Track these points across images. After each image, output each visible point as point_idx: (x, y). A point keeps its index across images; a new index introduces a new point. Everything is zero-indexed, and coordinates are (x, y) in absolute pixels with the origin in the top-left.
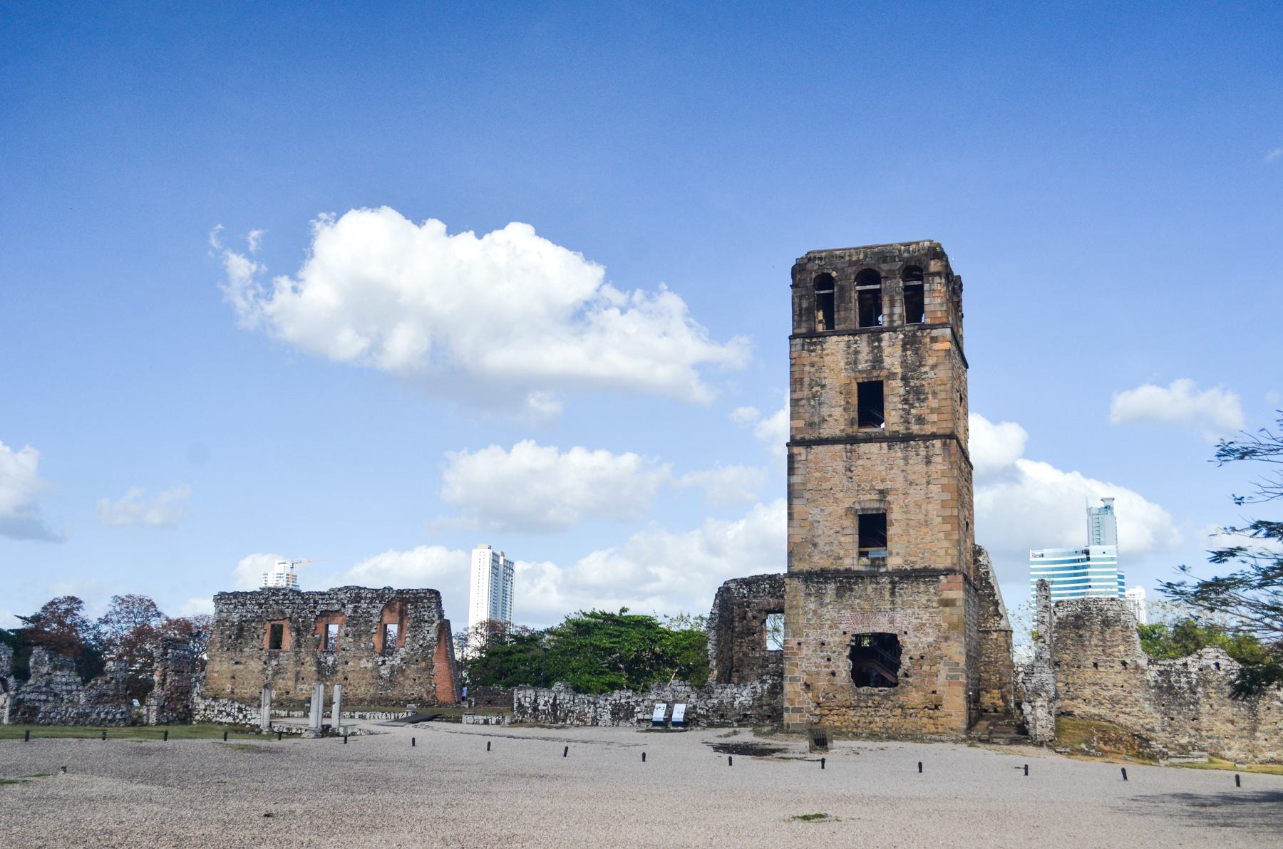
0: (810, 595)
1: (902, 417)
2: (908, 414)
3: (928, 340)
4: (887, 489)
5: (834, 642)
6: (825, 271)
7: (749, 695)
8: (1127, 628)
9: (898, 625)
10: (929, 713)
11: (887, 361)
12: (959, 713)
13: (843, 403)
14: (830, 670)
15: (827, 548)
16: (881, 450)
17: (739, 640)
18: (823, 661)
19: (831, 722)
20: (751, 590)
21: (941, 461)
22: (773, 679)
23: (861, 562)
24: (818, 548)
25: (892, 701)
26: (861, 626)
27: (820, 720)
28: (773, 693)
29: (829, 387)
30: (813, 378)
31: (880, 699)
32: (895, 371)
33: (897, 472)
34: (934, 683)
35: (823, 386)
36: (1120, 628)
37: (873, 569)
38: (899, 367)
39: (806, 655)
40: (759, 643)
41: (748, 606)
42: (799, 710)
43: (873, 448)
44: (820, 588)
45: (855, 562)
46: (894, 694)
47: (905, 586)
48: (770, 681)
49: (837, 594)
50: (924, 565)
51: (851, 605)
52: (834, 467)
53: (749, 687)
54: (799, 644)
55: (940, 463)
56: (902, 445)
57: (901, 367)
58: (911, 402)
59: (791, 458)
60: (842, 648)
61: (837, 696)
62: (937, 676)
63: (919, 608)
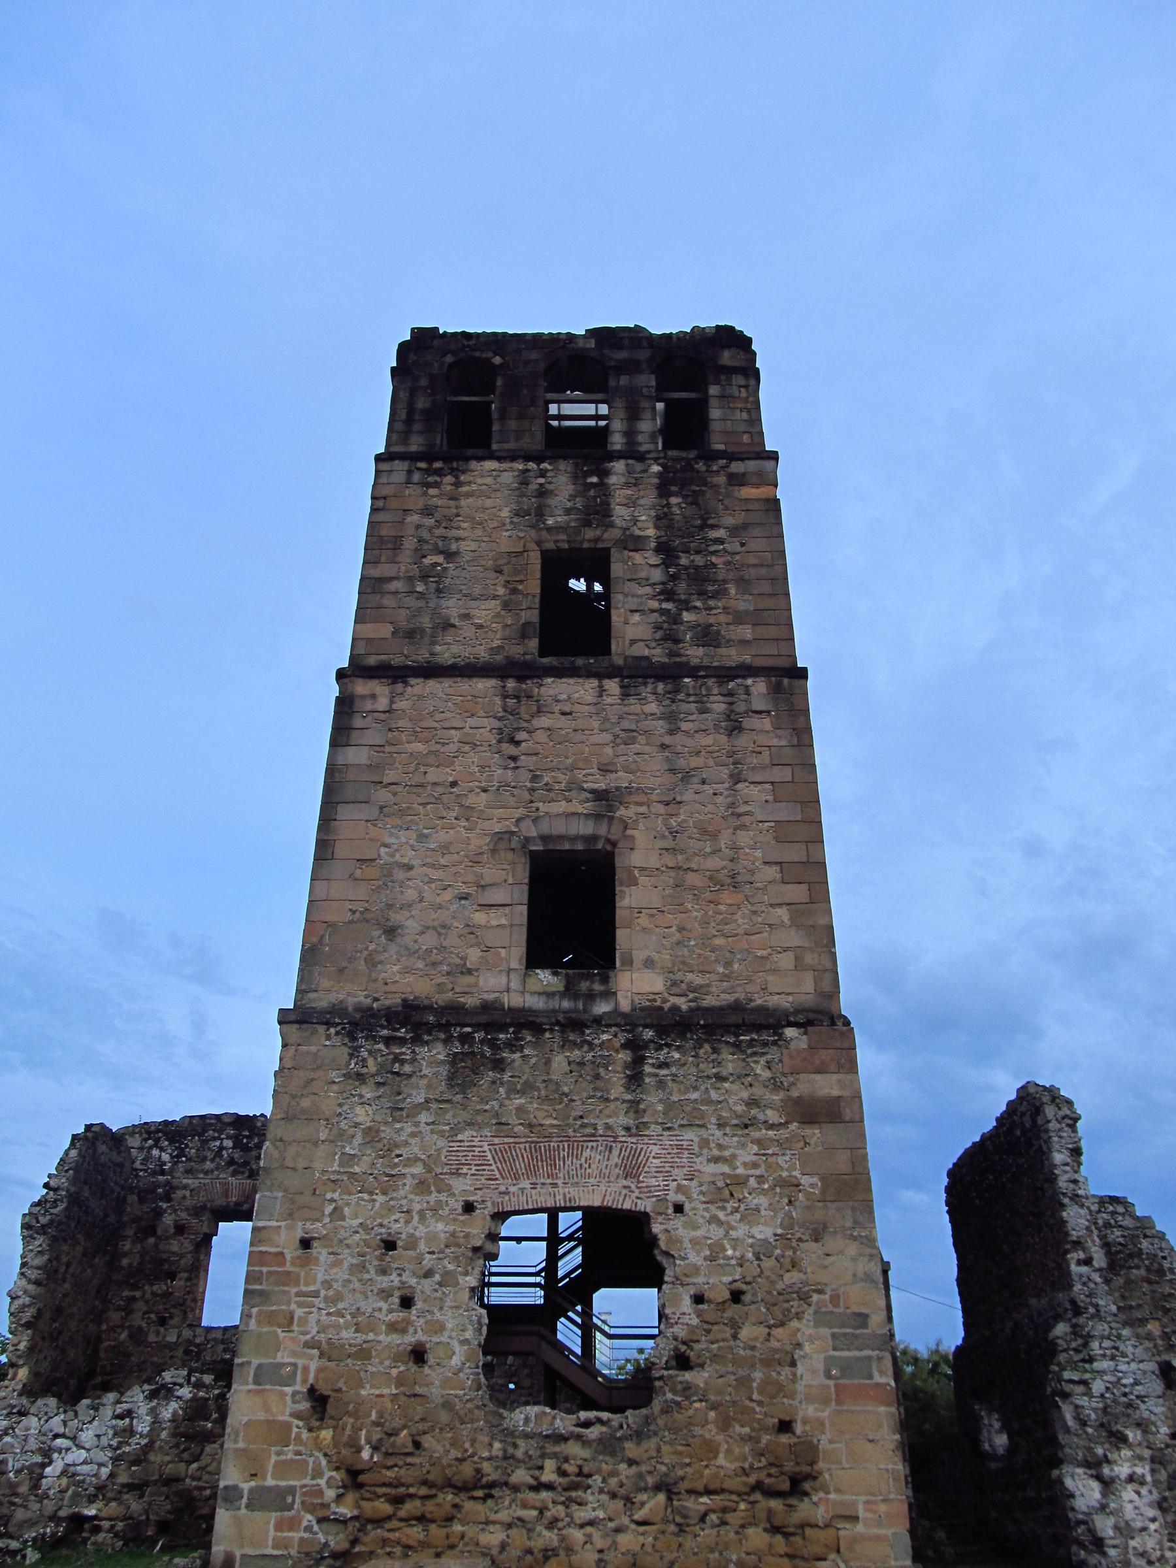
0: (360, 1078)
1: (658, 627)
2: (675, 623)
3: (721, 480)
4: (617, 789)
5: (432, 1237)
6: (477, 354)
7: (104, 1441)
8: (1161, 1272)
9: (653, 1182)
10: (770, 1511)
11: (620, 513)
12: (883, 1508)
13: (501, 591)
14: (410, 1339)
15: (429, 941)
16: (601, 696)
17: (126, 1293)
18: (385, 1306)
19: (398, 1550)
20: (182, 1153)
21: (768, 727)
22: (199, 1385)
23: (532, 984)
24: (399, 940)
25: (631, 1462)
26: (525, 1184)
27: (354, 1542)
28: (190, 1437)
29: (468, 558)
30: (425, 535)
31: (586, 1453)
32: (641, 533)
33: (647, 749)
34: (780, 1388)
35: (450, 556)
36: (1143, 1272)
37: (566, 1004)
38: (651, 525)
39: (327, 1284)
40: (181, 1304)
41: (167, 1198)
42: (276, 1500)
43: (582, 690)
44: (397, 1059)
45: (515, 984)
46: (639, 1435)
47: (677, 1055)
48: (185, 1392)
49: (451, 1078)
50: (728, 998)
51: (497, 1115)
52: (467, 730)
53: (108, 1412)
54: (306, 1244)
55: (768, 732)
56: (661, 687)
57: (657, 527)
58: (683, 597)
59: (345, 707)
60: (456, 1258)
61: (427, 1441)
62: (793, 1364)
63: (720, 1126)
